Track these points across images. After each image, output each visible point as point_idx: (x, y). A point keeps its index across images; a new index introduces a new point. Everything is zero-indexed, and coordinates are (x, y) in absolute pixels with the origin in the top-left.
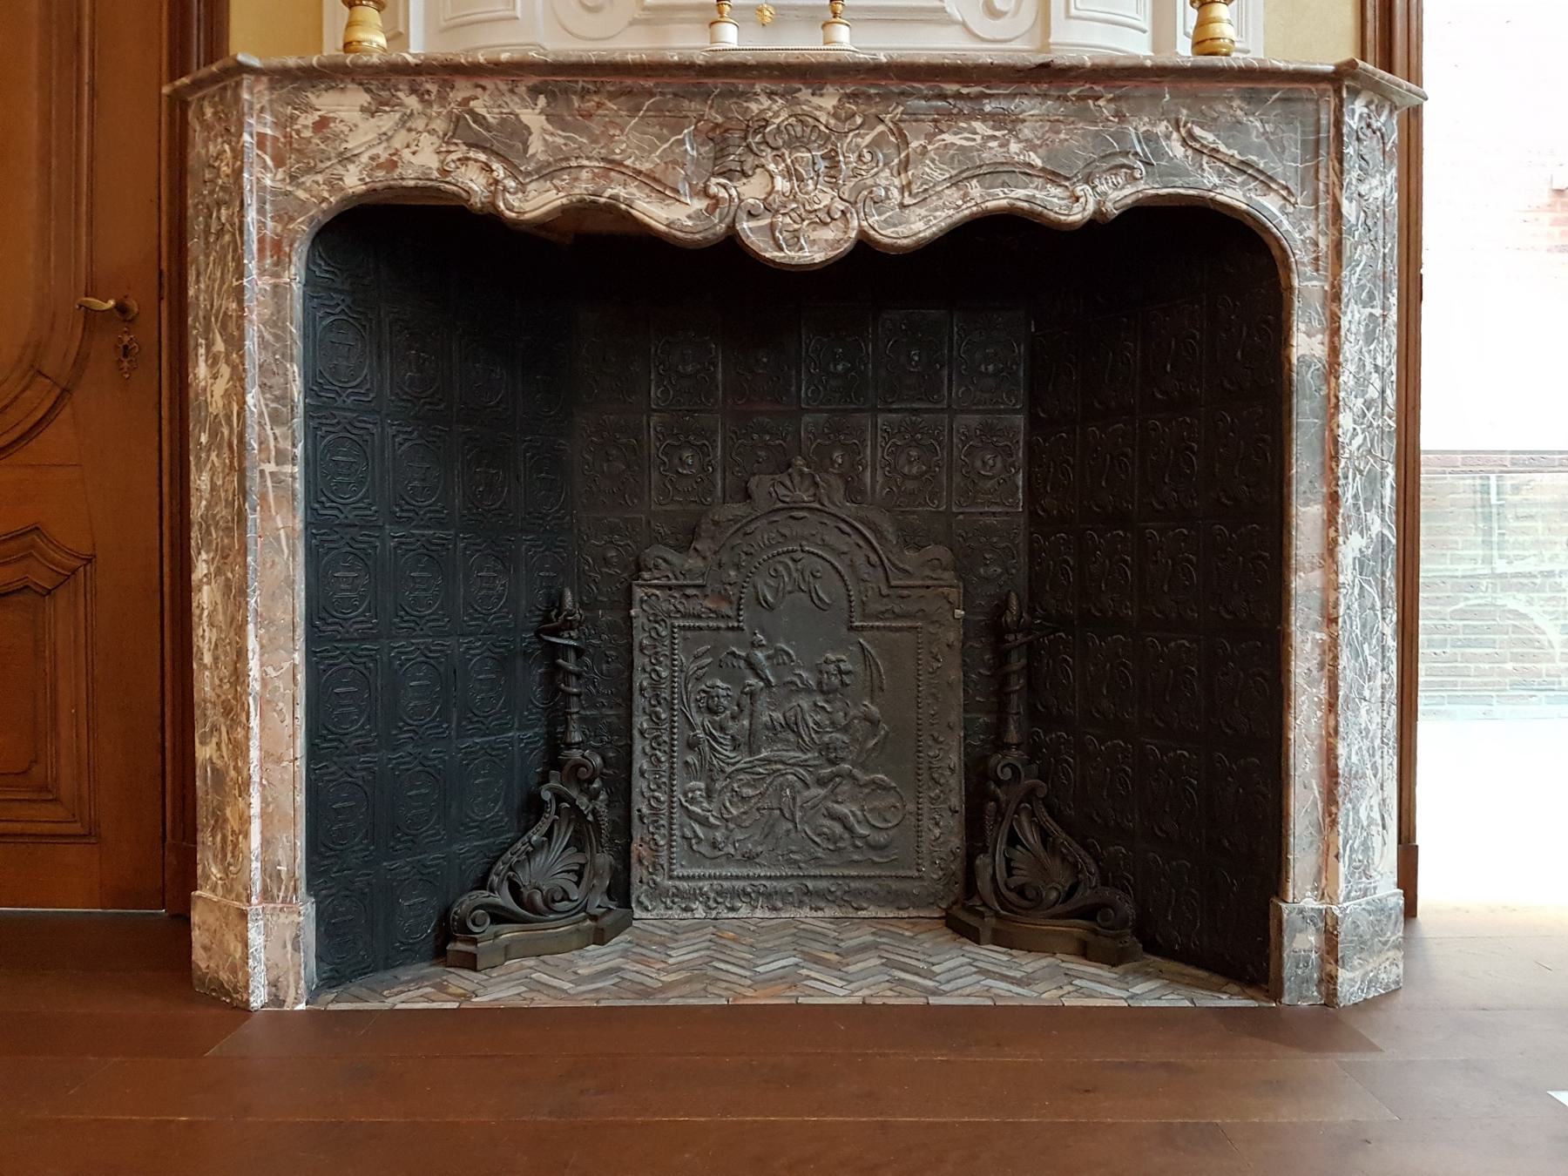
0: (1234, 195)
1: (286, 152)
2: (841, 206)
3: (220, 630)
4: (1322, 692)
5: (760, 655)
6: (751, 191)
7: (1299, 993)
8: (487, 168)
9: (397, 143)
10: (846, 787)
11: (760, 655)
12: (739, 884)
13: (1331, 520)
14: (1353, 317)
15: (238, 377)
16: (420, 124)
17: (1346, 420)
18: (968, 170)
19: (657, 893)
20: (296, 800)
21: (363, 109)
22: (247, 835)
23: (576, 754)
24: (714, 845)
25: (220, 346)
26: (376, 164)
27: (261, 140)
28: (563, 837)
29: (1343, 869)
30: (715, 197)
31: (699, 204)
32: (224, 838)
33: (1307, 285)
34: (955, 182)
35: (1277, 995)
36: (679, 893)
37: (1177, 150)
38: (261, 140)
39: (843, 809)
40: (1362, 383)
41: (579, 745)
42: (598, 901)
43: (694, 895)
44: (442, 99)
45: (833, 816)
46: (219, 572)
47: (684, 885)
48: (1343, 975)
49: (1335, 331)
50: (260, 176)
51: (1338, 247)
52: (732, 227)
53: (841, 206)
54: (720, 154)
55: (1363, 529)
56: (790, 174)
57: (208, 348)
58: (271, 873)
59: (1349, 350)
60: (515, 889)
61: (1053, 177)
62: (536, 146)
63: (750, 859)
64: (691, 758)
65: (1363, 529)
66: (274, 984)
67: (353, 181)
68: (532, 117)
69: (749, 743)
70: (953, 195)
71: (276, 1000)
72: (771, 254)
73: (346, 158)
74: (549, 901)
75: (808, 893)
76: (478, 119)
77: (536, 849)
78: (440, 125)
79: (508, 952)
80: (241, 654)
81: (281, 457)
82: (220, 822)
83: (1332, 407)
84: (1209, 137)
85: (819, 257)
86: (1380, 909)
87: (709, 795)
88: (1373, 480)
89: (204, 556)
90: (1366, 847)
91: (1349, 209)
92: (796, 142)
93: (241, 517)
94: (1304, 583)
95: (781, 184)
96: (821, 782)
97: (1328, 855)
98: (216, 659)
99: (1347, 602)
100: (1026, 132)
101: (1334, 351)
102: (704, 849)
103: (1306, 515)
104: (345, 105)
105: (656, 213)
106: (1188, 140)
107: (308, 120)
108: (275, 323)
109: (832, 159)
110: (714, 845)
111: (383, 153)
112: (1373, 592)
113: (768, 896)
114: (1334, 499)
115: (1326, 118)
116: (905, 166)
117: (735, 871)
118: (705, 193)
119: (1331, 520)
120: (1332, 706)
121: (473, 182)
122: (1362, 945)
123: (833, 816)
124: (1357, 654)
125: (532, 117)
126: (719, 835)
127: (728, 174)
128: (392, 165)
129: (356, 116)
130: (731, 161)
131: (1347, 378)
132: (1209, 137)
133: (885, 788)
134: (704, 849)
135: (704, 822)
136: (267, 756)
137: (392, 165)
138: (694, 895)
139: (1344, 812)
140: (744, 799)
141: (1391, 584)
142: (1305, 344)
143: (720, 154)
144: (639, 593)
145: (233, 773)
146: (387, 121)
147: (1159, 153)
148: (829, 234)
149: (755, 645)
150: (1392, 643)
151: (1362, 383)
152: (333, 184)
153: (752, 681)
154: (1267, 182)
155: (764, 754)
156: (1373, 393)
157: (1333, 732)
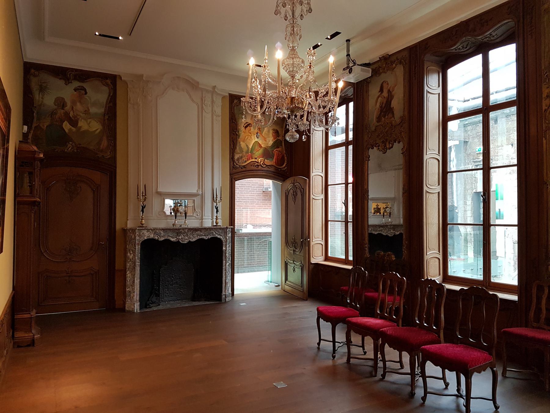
0: (219, 237)
1: (139, 236)
2: (188, 238)
3: (130, 278)
4: (225, 276)
5: (173, 276)
6: (180, 237)
7: (223, 301)
8: (158, 236)
9: (149, 234)
10: (182, 288)
11: (173, 276)
12: (171, 299)
13: (226, 262)
14: (228, 246)
15: (134, 256)
16: (152, 233)
17: (227, 254)
18: (198, 235)
19: (162, 301)
20: (138, 293)
21: (147, 232)
22: (134, 297)
23: (155, 287)
24: (168, 296)
25: (131, 252)
26: (148, 237)
27: (137, 235)
28: (154, 296)
29: (227, 290)
30: (177, 238)
31: (176, 239)
32: (130, 297)
33: (224, 244)
34: (197, 236)
35: (221, 301)
36: (165, 301)
37: (214, 233)
38: (137, 235)
39: (181, 291)
40: (228, 251)
41: (155, 286)
42: (158, 302)
43: (166, 301)
44: (154, 230)
45: (180, 291)
46: (130, 273)
47: (165, 300)
48: (226, 299)
49: (226, 247)
50: (137, 238)
51: (226, 241)
52: (179, 241)
53: (188, 238)
54: (178, 234)
55: (228, 263)
56: (183, 236)
57: (130, 252)
58: (136, 300)
59: (227, 249)
60: (151, 301)
61: (205, 236)
62: (162, 235)
63: (172, 297)
64: (166, 287)
65: (228, 263)
66: (137, 310)
67: (146, 238)
68: (162, 232)
69: (172, 285)
70: (197, 237)
71: (137, 311)
72: (182, 242)
73: (145, 236)
74: (155, 302)
75: (178, 299)
76: (157, 232)
77: (152, 297)
78: (153, 233)
79: (152, 307)
80: (134, 280)
81: (138, 262)
82: (130, 296)
83: (226, 254)
84: (217, 232)
85: (186, 243)
86: (230, 293)
87: (168, 290)
88: (229, 258)
89: (128, 271)
90: (228, 288)
91: (227, 238)
92: (184, 233)
93: (135, 268)
94: (224, 267)
95: (183, 237)
96: (179, 288)
97: (226, 289)
98: (130, 281)
99: (227, 269)
100: (203, 232)
101: (226, 249)
102: (167, 296)
103: (224, 262)
104: (145, 232)
105: (172, 240)
106: (215, 232)
107: (142, 233)
108: (138, 250)
109: (187, 235)
110: (168, 296)
111: (148, 235)
112: (229, 267)
113: (174, 300)
114: (226, 261)
115: (226, 230)
116: (193, 235)
117: (170, 298)
118: (176, 238)
119: (226, 262)
120: (226, 277)
121: (157, 238)
122: (228, 296)
123: (180, 291)
124: (228, 273)
125: (162, 232)
126: (169, 295)
127: (178, 236)
128: (149, 236)
129: (146, 232)
130: (179, 235)
131: (227, 251)
132: (217, 232)
133: (186, 288)
134: (167, 296)
135: (167, 293)
136: (136, 289)
137: (149, 236)
138: (166, 301)
139: (227, 285)
140: (171, 291)
141: (230, 267)
142: (224, 248)
143: (178, 234)
144: (161, 270)
145: (132, 291)
146: (149, 233)
147: (213, 234)
148: (187, 241)
149: (173, 275)
150: (231, 271)
151: (228, 251)
152: (144, 238)
153: (173, 278)
154: (221, 236)
155: (173, 286)
156: (229, 251)
157: (226, 279)
